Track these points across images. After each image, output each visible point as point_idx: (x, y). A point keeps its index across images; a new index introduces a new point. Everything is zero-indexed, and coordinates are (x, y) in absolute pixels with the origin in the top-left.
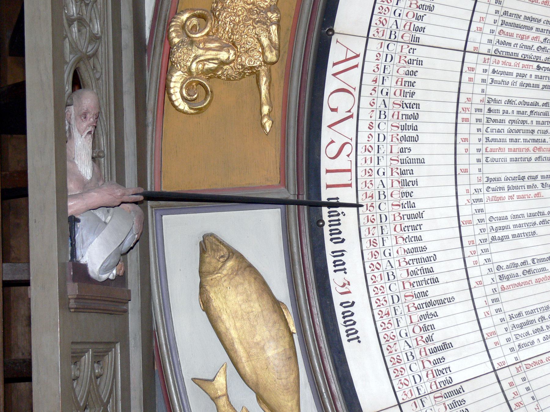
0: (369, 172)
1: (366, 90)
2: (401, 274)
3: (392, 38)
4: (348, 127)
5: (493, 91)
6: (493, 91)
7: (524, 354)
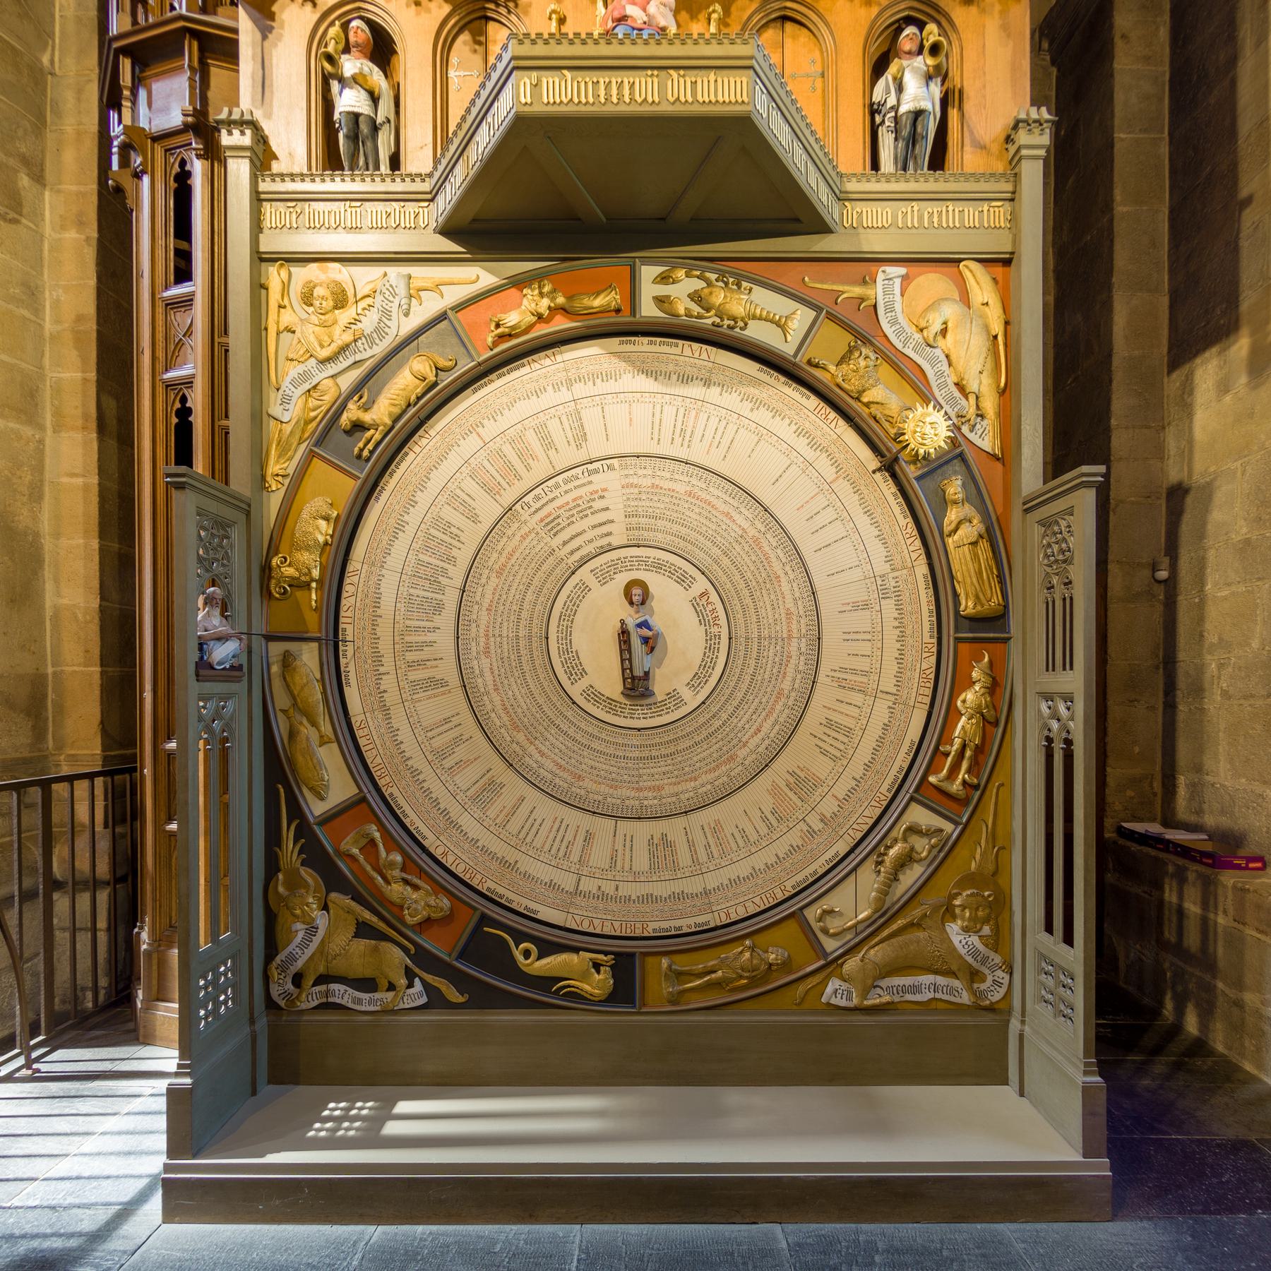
0: (359, 619)
1: (361, 585)
2: (370, 661)
3: (373, 565)
4: (352, 600)
5: (412, 591)
6: (412, 591)
7: (414, 697)
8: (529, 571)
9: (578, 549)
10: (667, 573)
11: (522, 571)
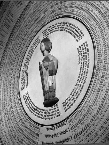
8: (92, 128)
9: (62, 133)
10: (31, 103)
11: (96, 129)
